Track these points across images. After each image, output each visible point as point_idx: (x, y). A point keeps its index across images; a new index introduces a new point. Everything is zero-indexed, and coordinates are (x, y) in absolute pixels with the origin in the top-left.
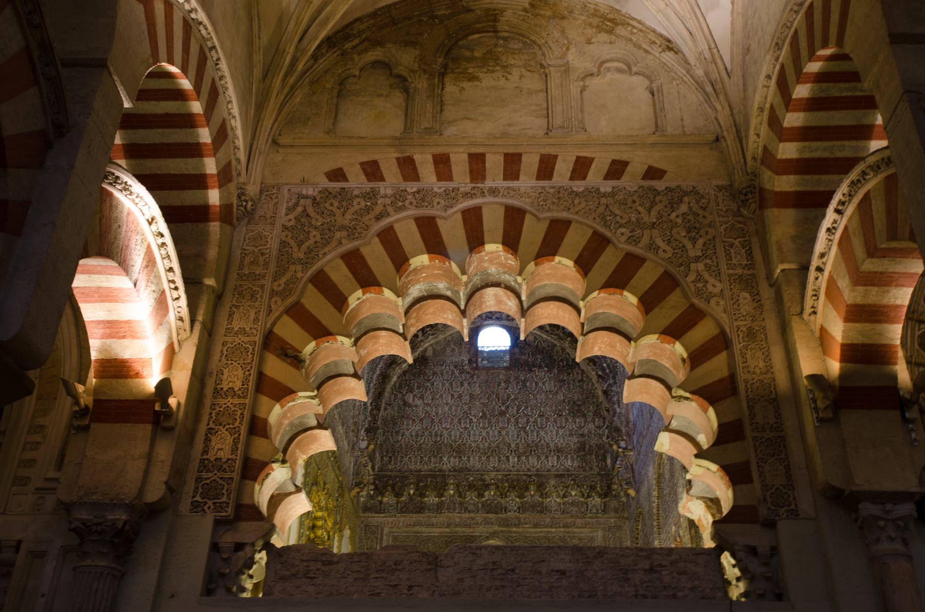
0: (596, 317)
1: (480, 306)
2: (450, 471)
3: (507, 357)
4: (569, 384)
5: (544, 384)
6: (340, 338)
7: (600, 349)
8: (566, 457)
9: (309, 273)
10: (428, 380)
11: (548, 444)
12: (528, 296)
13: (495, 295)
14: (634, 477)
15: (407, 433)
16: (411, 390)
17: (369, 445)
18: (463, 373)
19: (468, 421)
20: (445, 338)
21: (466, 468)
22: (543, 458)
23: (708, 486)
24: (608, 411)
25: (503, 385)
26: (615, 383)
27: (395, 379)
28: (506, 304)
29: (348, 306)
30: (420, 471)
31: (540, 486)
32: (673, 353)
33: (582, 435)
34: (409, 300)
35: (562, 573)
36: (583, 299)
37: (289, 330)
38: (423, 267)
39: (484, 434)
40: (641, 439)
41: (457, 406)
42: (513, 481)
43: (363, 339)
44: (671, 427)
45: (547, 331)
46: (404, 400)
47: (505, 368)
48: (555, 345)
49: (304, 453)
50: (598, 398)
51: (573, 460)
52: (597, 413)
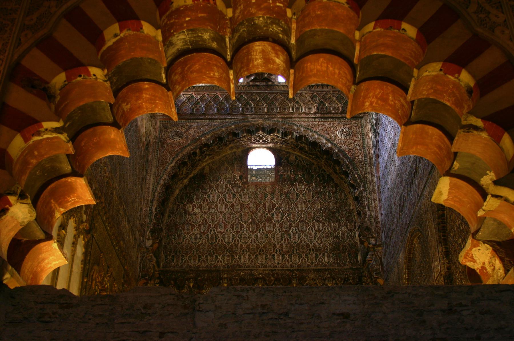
0: (371, 58)
1: (248, 65)
2: (224, 267)
3: (273, 174)
4: (325, 195)
5: (304, 195)
6: (94, 70)
7: (371, 103)
8: (323, 255)
9: (64, 8)
10: (206, 193)
11: (308, 244)
12: (297, 41)
13: (263, 52)
14: (382, 268)
15: (187, 236)
16: (191, 201)
17: (153, 243)
18: (235, 186)
19: (239, 226)
20: (220, 159)
21: (238, 265)
22: (304, 256)
23: (500, 224)
24: (359, 213)
25: (269, 196)
26: (365, 190)
27: (177, 191)
28: (274, 62)
29: (103, 42)
30: (198, 267)
31: (301, 280)
32: (457, 86)
33: (337, 237)
34: (172, 51)
35: (346, 316)
36: (359, 29)
37: (38, 62)
38: (186, 8)
39: (253, 236)
40: (390, 234)
41: (230, 214)
42: (278, 275)
43: (125, 90)
44: (452, 172)
45: (306, 152)
46: (185, 210)
47: (272, 184)
48: (313, 164)
49: (61, 205)
50: (350, 206)
51: (329, 257)
52: (349, 219)
